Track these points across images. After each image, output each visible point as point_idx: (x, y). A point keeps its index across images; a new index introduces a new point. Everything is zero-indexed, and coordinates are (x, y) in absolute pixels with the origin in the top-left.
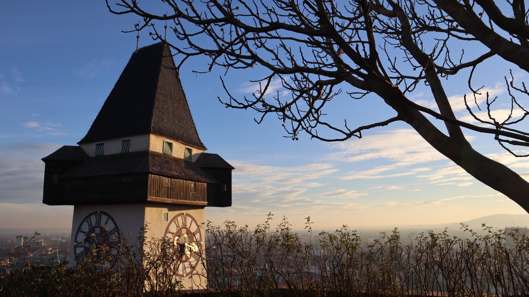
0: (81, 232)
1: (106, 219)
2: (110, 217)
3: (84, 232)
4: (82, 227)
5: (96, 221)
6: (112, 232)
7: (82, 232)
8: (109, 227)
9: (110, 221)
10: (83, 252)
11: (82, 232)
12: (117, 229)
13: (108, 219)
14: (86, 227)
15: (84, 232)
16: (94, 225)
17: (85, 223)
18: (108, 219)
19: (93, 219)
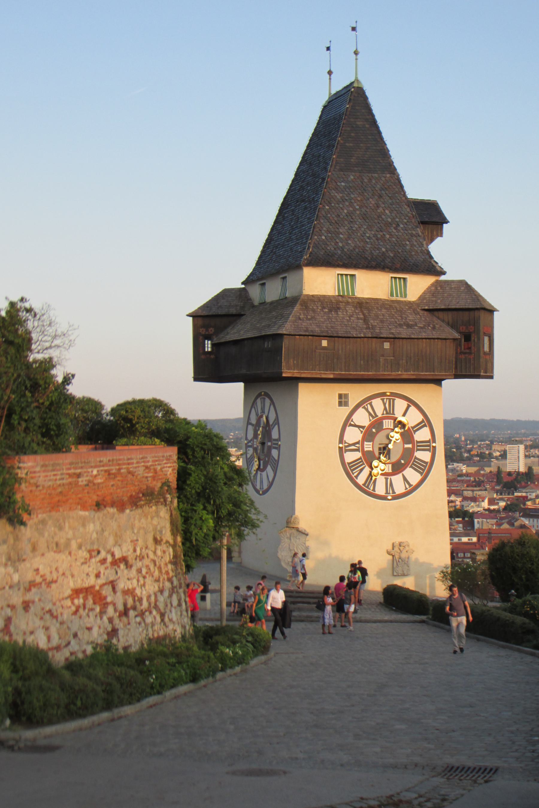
0: (351, 425)
1: (406, 406)
2: (411, 402)
3: (359, 427)
4: (354, 417)
5: (385, 409)
6: (419, 426)
7: (355, 426)
8: (412, 418)
9: (412, 408)
10: (360, 458)
11: (355, 426)
13: (408, 407)
14: (362, 418)
15: (359, 427)
16: (380, 415)
17: (361, 410)
18: (408, 407)
19: (378, 405)
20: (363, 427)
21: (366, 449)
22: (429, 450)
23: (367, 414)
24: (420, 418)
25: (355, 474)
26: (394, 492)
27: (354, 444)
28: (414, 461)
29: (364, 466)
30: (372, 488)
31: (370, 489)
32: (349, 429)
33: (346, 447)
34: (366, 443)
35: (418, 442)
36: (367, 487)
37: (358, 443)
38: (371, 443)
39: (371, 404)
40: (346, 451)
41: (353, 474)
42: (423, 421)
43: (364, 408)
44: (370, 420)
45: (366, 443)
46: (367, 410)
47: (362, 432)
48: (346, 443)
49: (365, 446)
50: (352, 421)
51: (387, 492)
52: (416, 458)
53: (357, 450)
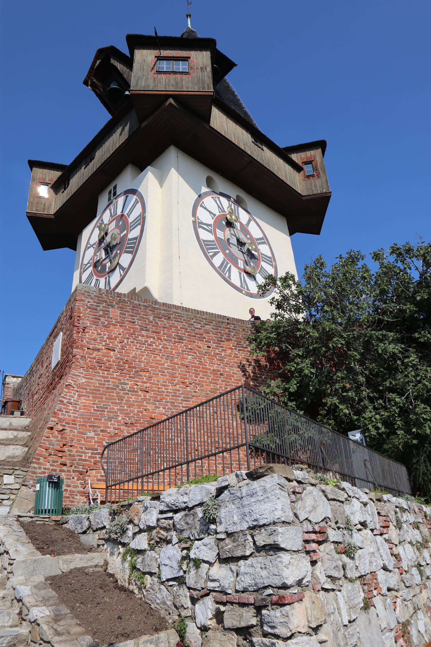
0: (201, 206)
8: (255, 232)
11: (206, 208)
12: (265, 240)
20: (215, 215)
21: (218, 236)
22: (272, 265)
23: (217, 205)
24: (261, 235)
25: (211, 254)
26: (248, 289)
27: (207, 225)
28: (261, 269)
29: (217, 250)
30: (227, 275)
31: (225, 274)
32: (200, 209)
33: (199, 223)
34: (217, 230)
35: (262, 254)
36: (223, 271)
37: (210, 225)
38: (223, 233)
39: (219, 198)
40: (200, 227)
41: (209, 253)
42: (262, 239)
43: (213, 198)
44: (220, 212)
45: (217, 230)
46: (216, 201)
47: (213, 218)
48: (198, 219)
49: (217, 233)
50: (203, 202)
51: (241, 286)
52: (262, 267)
53: (210, 232)
